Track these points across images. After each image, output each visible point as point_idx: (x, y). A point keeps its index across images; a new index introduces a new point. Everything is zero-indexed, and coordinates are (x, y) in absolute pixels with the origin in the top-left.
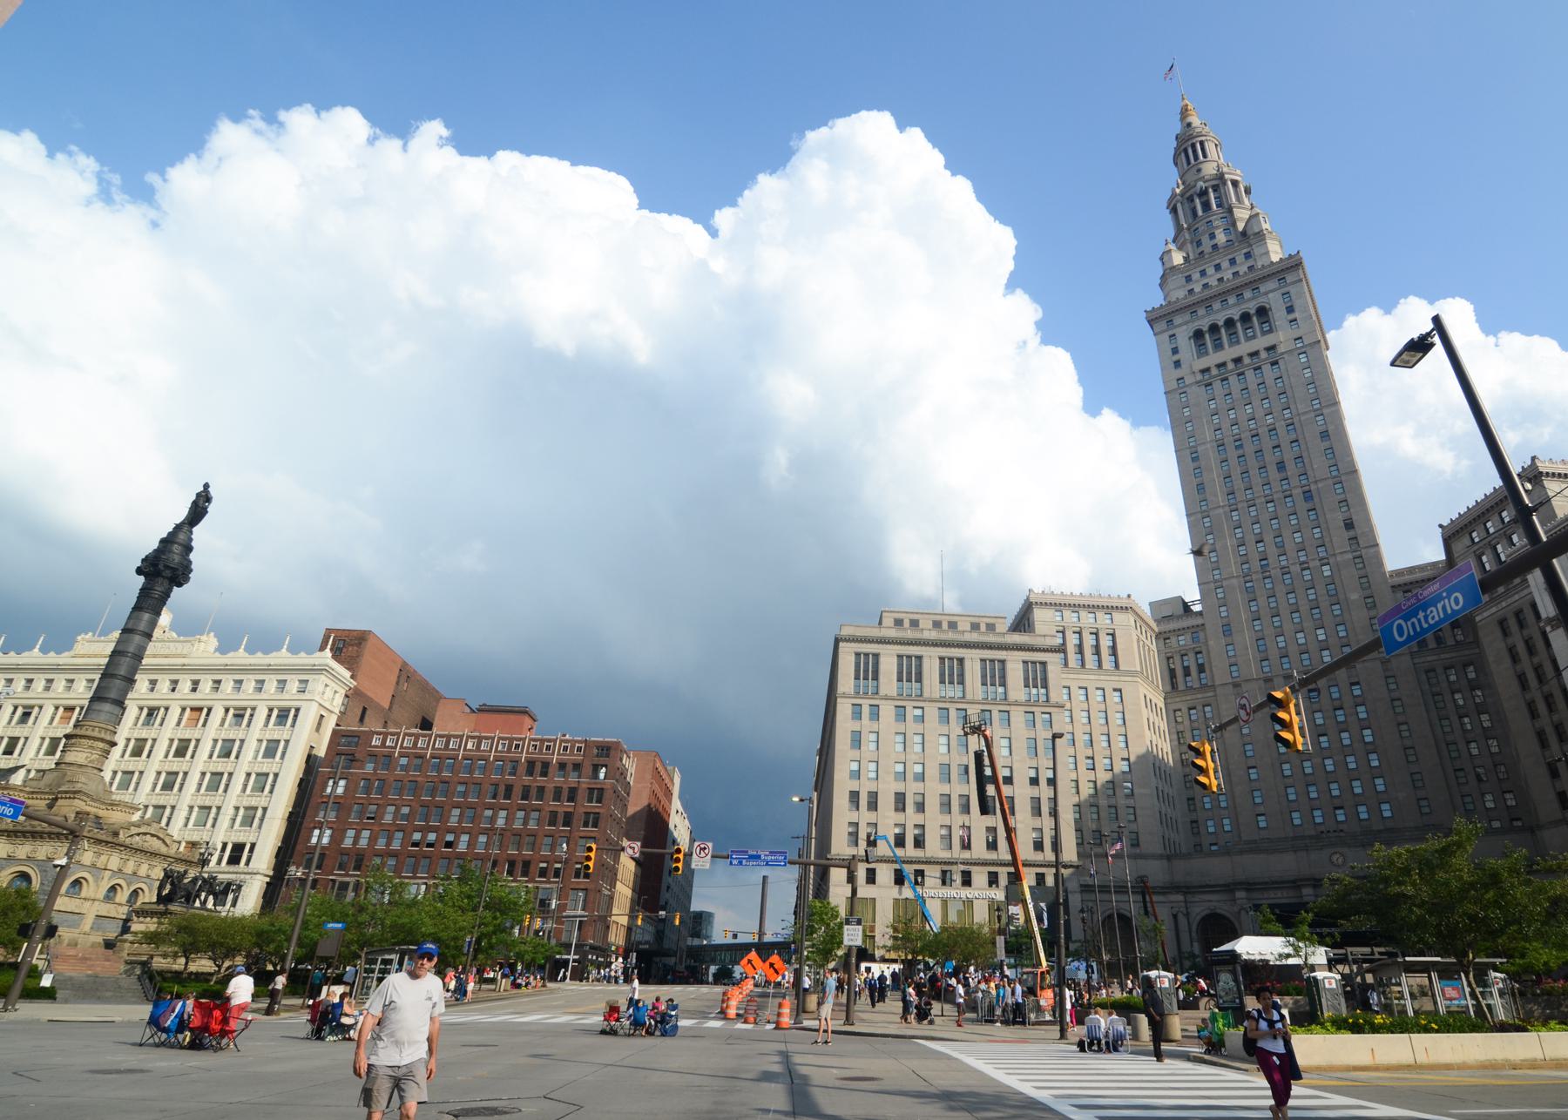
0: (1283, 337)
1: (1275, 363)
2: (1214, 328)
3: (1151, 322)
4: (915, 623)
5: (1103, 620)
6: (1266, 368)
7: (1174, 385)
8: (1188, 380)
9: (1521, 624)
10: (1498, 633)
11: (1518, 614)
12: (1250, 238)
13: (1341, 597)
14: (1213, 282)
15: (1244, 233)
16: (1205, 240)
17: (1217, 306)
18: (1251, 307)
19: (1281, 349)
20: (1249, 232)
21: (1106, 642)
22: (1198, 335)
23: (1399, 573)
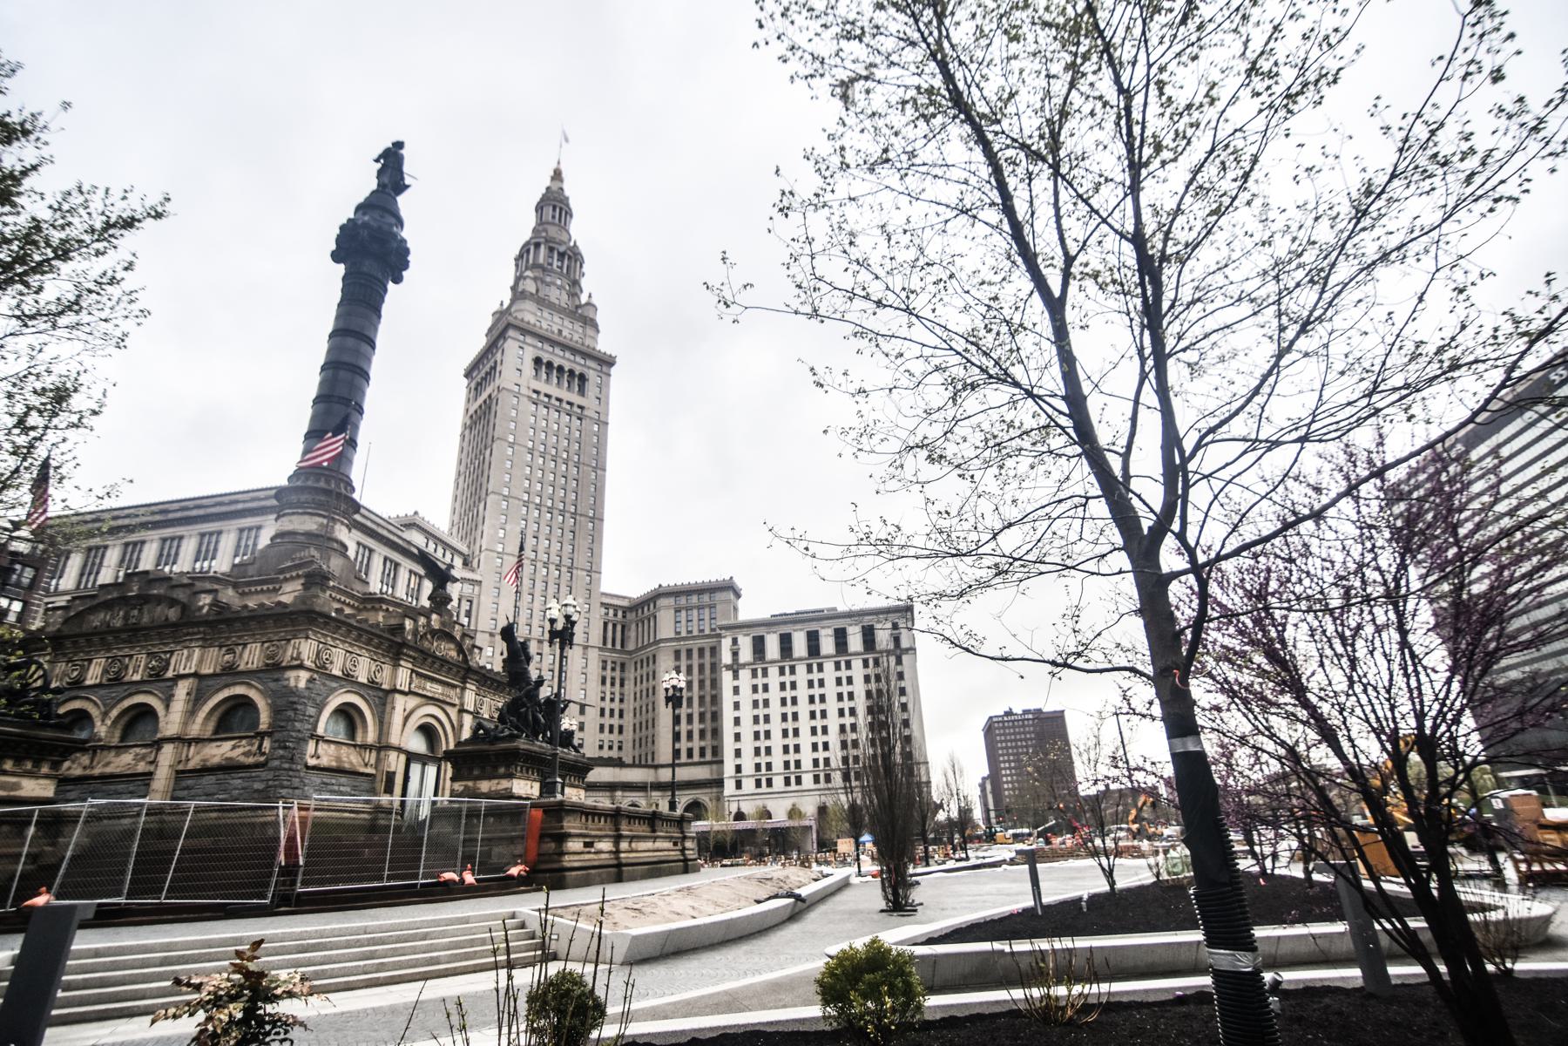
0: (589, 401)
2: (549, 365)
8: (524, 391)
10: (672, 657)
18: (578, 370)
22: (538, 361)
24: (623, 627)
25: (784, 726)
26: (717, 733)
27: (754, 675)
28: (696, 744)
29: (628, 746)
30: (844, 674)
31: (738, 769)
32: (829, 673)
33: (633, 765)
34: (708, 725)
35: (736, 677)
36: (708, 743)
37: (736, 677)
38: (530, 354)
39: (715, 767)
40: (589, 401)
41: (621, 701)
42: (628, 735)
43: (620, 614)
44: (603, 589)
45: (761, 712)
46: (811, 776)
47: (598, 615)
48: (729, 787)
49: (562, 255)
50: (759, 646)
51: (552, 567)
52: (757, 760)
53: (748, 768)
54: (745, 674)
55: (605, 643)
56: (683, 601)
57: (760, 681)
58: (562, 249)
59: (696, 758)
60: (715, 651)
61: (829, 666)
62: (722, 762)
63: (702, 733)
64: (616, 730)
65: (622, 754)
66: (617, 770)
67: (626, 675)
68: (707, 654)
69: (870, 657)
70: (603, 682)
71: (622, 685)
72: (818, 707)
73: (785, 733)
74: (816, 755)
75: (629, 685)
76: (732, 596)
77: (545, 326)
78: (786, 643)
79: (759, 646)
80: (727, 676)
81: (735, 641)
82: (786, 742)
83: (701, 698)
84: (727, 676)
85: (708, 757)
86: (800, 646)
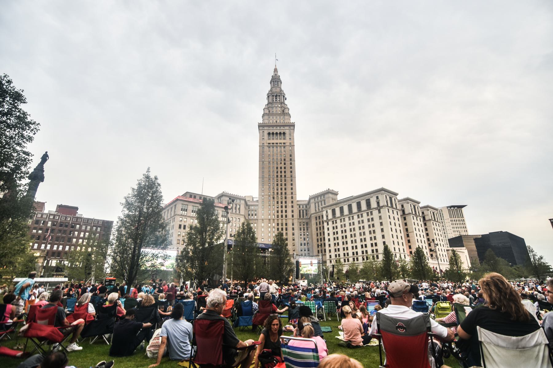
2: (273, 133)
3: (259, 126)
4: (195, 197)
8: (265, 144)
9: (319, 218)
10: (315, 219)
12: (285, 113)
16: (274, 108)
22: (269, 134)
23: (298, 201)
24: (306, 211)
30: (360, 219)
32: (356, 220)
37: (328, 224)
38: (266, 132)
40: (287, 141)
43: (305, 207)
44: (298, 199)
53: (333, 257)
54: (330, 223)
55: (300, 217)
57: (335, 225)
58: (275, 94)
62: (326, 255)
67: (309, 226)
70: (301, 230)
76: (330, 195)
77: (271, 122)
80: (325, 224)
81: (327, 212)
84: (325, 224)
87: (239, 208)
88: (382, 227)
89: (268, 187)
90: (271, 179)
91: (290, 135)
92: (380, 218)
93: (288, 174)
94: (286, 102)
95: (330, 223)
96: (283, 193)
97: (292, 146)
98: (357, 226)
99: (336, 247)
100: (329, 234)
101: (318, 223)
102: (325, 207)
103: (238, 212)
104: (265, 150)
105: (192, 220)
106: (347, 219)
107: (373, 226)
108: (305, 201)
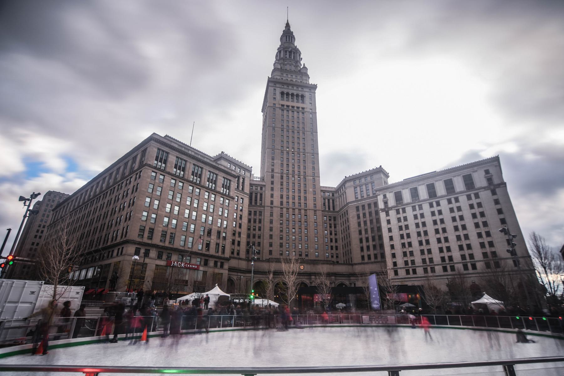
1: (303, 113)
2: (288, 94)
3: (270, 81)
5: (243, 172)
6: (300, 113)
7: (272, 105)
8: (277, 106)
10: (355, 210)
11: (363, 206)
13: (307, 189)
14: (289, 79)
15: (300, 71)
17: (290, 87)
19: (305, 110)
20: (302, 71)
21: (241, 180)
22: (282, 93)
24: (333, 201)
25: (419, 239)
26: (382, 246)
27: (398, 212)
28: (372, 252)
29: (341, 256)
30: (454, 205)
31: (395, 264)
33: (344, 264)
34: (377, 242)
35: (388, 215)
36: (378, 251)
38: (278, 91)
39: (383, 264)
40: (307, 105)
41: (336, 234)
42: (341, 251)
43: (331, 195)
44: (321, 185)
45: (404, 232)
46: (441, 267)
47: (319, 196)
48: (391, 274)
49: (290, 52)
50: (398, 197)
51: (296, 177)
52: (406, 259)
54: (392, 213)
56: (357, 182)
58: (290, 50)
59: (373, 259)
60: (376, 204)
61: (444, 202)
62: (385, 262)
63: (375, 247)
64: (334, 248)
65: (339, 260)
66: (332, 266)
67: (337, 222)
68: (373, 206)
69: (472, 193)
71: (335, 227)
72: (440, 226)
73: (421, 243)
74: (442, 255)
75: (339, 228)
76: (382, 176)
78: (415, 193)
79: (398, 197)
81: (385, 196)
82: (422, 248)
83: (372, 229)
85: (379, 259)
86: (423, 193)
87: (243, 183)
88: (502, 216)
89: (280, 162)
90: (285, 152)
91: (311, 99)
92: (497, 202)
93: (309, 149)
94: (302, 62)
95: (392, 213)
96: (302, 173)
97: (314, 113)
98: (447, 215)
99: (405, 250)
100: (390, 230)
101: (361, 215)
102: (380, 190)
103: (241, 189)
104: (277, 113)
105: (173, 181)
106: (426, 206)
107: (482, 214)
108: (332, 188)
